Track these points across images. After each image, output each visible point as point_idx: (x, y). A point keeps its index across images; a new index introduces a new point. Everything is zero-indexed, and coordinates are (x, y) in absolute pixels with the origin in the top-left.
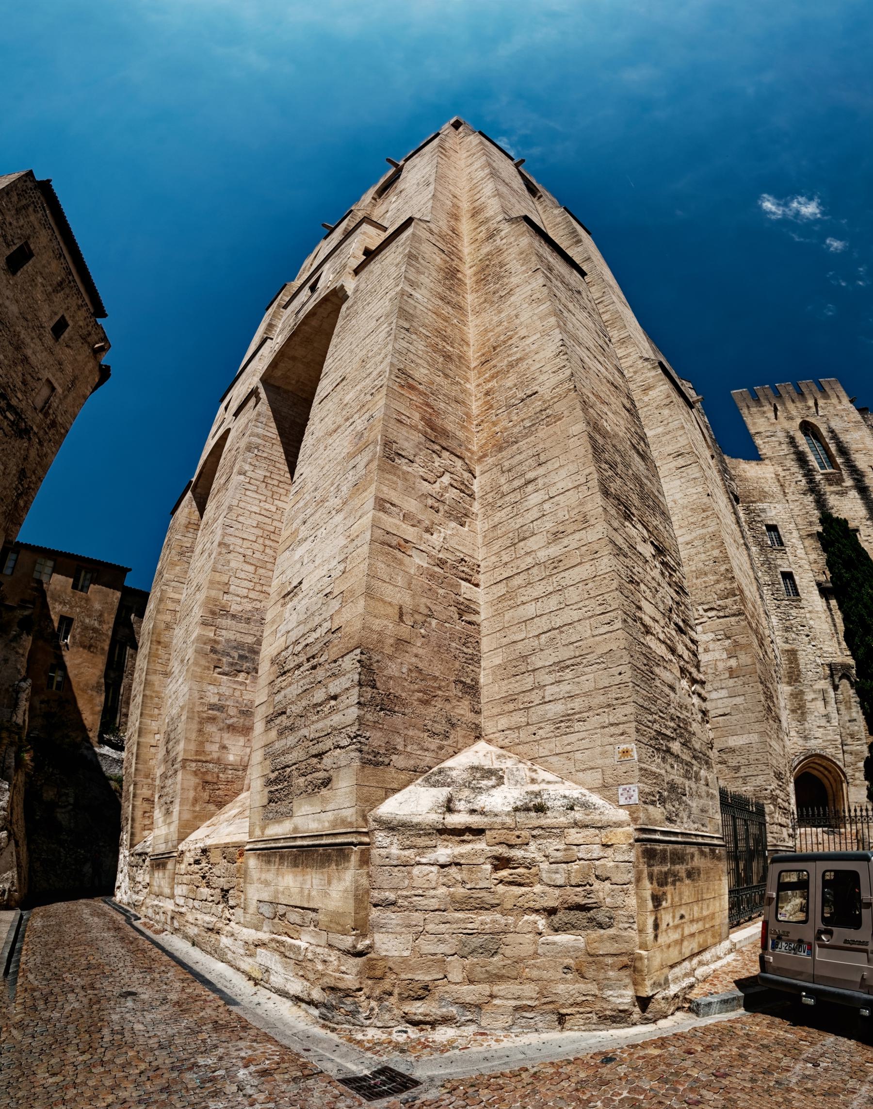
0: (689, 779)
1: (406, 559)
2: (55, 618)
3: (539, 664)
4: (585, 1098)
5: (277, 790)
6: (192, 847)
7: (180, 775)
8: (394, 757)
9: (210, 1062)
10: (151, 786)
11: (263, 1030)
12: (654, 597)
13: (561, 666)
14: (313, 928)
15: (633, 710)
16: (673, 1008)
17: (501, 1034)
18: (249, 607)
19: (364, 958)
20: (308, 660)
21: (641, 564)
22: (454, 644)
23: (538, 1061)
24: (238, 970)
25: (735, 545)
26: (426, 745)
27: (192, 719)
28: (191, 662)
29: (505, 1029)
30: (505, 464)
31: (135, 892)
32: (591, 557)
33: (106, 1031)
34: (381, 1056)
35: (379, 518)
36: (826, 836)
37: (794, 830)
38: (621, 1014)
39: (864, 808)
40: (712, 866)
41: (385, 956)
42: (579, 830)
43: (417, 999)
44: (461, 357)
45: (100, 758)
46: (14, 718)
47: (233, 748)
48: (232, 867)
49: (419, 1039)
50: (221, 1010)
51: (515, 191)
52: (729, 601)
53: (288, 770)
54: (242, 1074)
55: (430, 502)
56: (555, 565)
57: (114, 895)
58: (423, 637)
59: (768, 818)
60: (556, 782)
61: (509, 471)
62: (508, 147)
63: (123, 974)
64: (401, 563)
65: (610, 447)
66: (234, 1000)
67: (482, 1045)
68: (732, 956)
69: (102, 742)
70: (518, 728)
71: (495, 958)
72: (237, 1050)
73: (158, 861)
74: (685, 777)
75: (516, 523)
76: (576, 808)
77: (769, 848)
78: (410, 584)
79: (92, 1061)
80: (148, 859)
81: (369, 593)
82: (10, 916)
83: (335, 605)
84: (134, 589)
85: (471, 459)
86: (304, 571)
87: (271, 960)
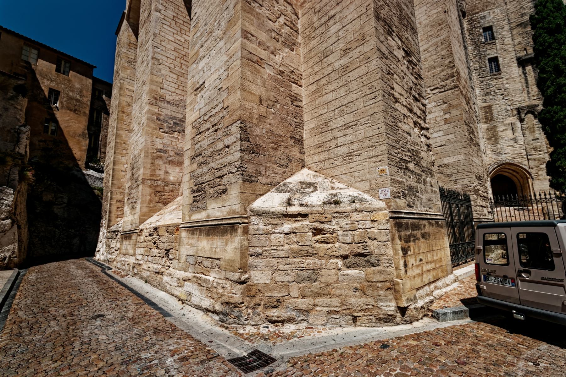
0: (420, 183)
1: (262, 70)
3: (335, 126)
4: (373, 372)
5: (198, 196)
6: (148, 227)
7: (140, 188)
8: (260, 178)
9: (149, 355)
10: (122, 193)
11: (185, 331)
12: (402, 82)
13: (346, 127)
14: (217, 269)
15: (386, 148)
16: (421, 315)
17: (320, 327)
19: (245, 285)
20: (213, 126)
21: (395, 62)
22: (289, 117)
23: (343, 346)
24: (173, 295)
26: (276, 171)
27: (148, 156)
28: (145, 125)
29: (323, 325)
31: (109, 253)
33: (77, 344)
34: (253, 343)
35: (245, 43)
36: (517, 212)
37: (492, 209)
38: (389, 317)
39: (547, 193)
40: (437, 231)
41: (257, 283)
42: (358, 213)
43: (274, 307)
45: (87, 177)
46: (17, 149)
47: (172, 173)
48: (172, 237)
49: (275, 332)
50: (160, 320)
53: (204, 185)
54: (169, 361)
55: (273, 35)
56: (344, 69)
57: (94, 256)
58: (273, 114)
59: (472, 203)
60: (345, 188)
61: (319, 11)
63: (96, 304)
64: (259, 72)
66: (169, 314)
67: (310, 335)
68: (456, 285)
69: (88, 167)
70: (324, 161)
71: (316, 283)
72: (168, 345)
73: (126, 235)
74: (418, 182)
75: (322, 47)
76: (356, 202)
77: (475, 220)
79: (61, 367)
80: (119, 234)
82: (9, 274)
83: (224, 94)
85: (296, 5)
87: (193, 288)
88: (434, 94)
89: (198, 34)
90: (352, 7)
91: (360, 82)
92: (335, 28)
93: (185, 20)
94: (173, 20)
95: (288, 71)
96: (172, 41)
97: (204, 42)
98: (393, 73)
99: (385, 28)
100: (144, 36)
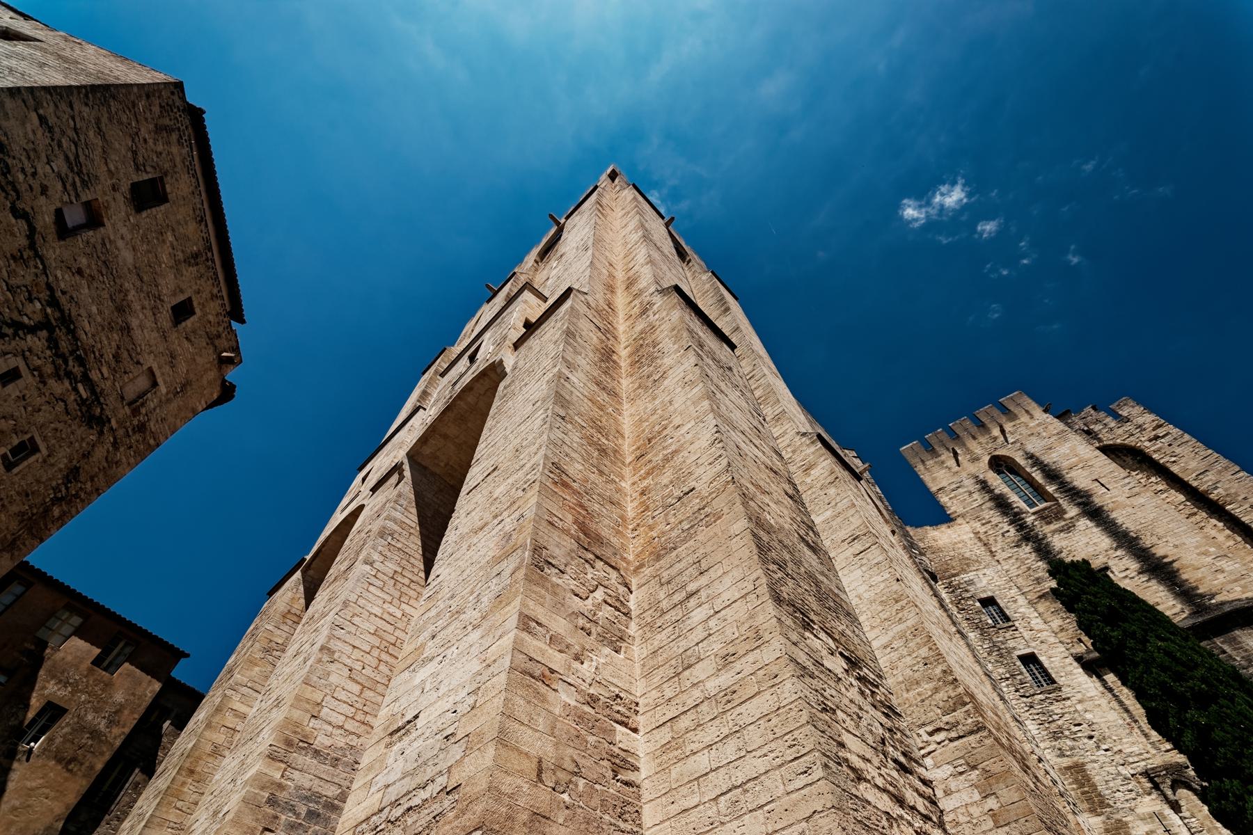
1: (551, 694)
2: (36, 703)
12: (858, 726)
18: (341, 742)
21: (833, 684)
22: (607, 817)
25: (946, 636)
30: (664, 574)
32: (771, 683)
35: (522, 640)
44: (616, 451)
51: (665, 256)
52: (959, 714)
55: (581, 622)
62: (659, 202)
65: (775, 544)
75: (678, 647)
78: (553, 728)
81: (502, 740)
84: (184, 685)
86: (424, 701)
88: (939, 743)
89: (433, 613)
90: (728, 581)
91: (766, 729)
92: (701, 612)
93: (415, 578)
94: (392, 578)
95: (607, 695)
96: (376, 616)
97: (439, 629)
98: (835, 708)
99: (796, 617)
100: (323, 604)
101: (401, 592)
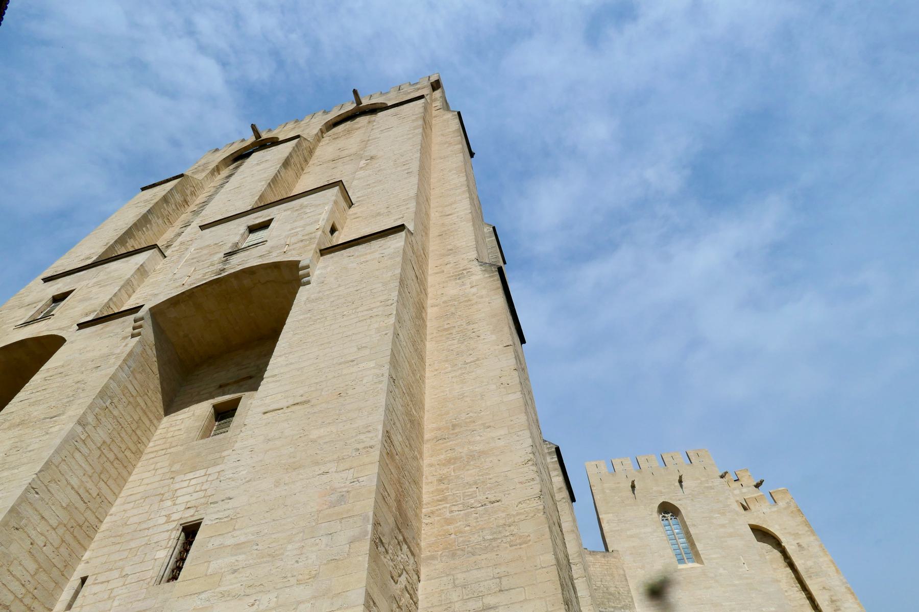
94: (99, 448)
96: (73, 488)
101: (104, 468)
